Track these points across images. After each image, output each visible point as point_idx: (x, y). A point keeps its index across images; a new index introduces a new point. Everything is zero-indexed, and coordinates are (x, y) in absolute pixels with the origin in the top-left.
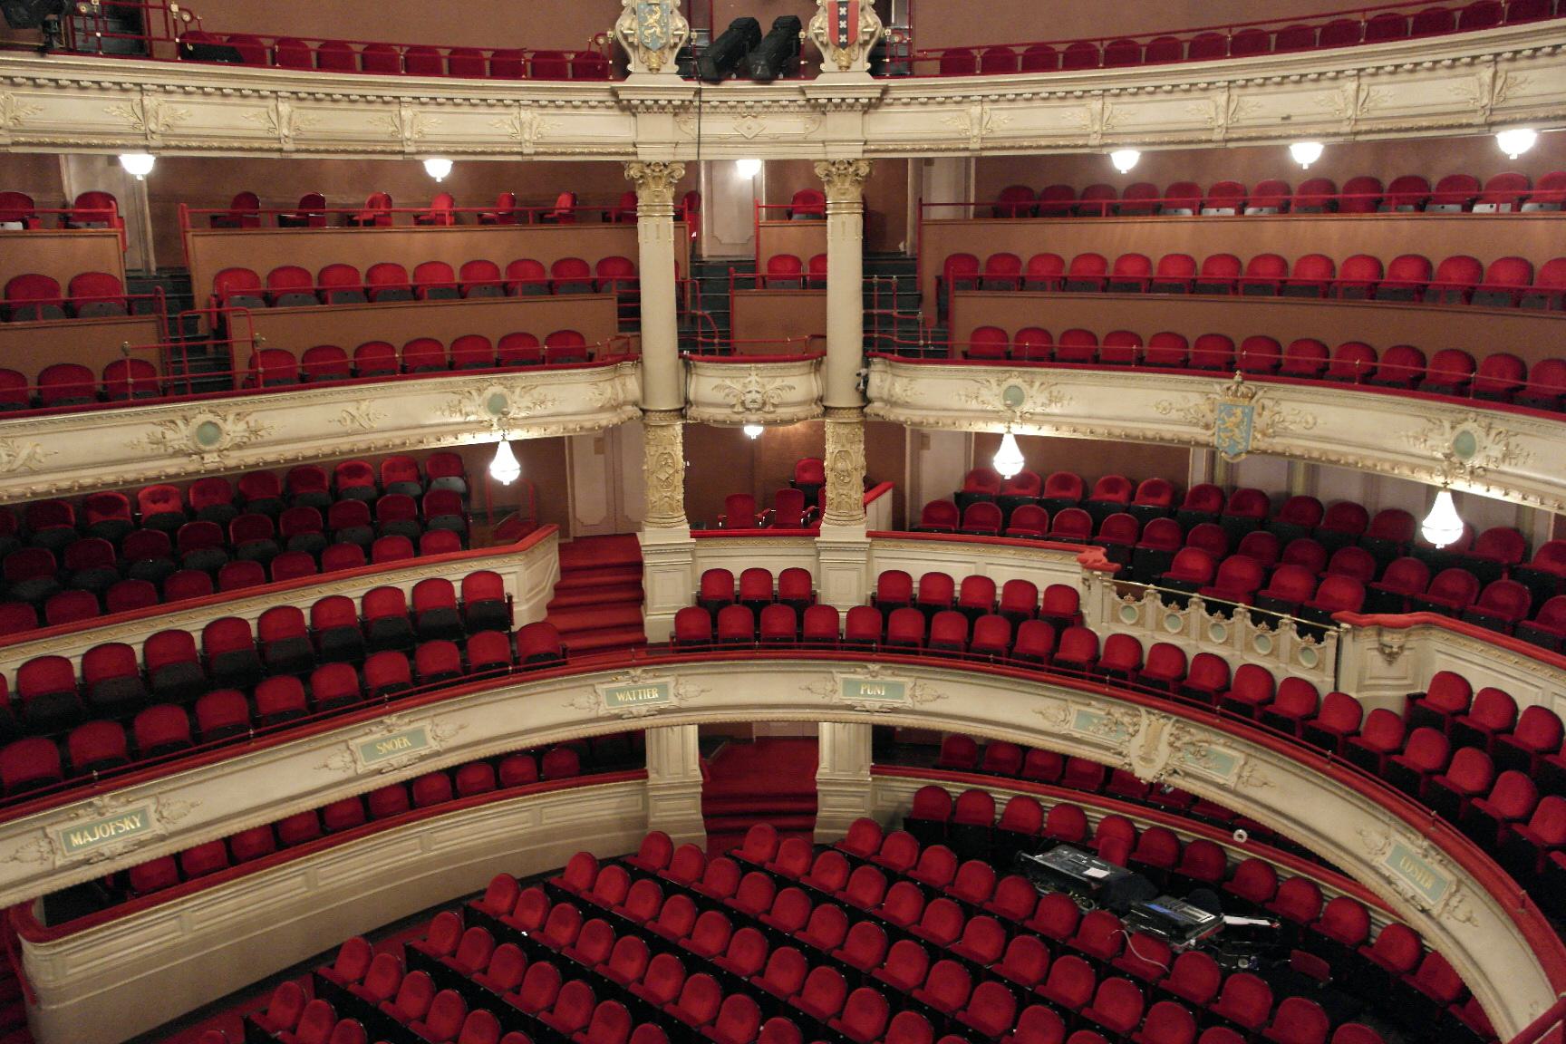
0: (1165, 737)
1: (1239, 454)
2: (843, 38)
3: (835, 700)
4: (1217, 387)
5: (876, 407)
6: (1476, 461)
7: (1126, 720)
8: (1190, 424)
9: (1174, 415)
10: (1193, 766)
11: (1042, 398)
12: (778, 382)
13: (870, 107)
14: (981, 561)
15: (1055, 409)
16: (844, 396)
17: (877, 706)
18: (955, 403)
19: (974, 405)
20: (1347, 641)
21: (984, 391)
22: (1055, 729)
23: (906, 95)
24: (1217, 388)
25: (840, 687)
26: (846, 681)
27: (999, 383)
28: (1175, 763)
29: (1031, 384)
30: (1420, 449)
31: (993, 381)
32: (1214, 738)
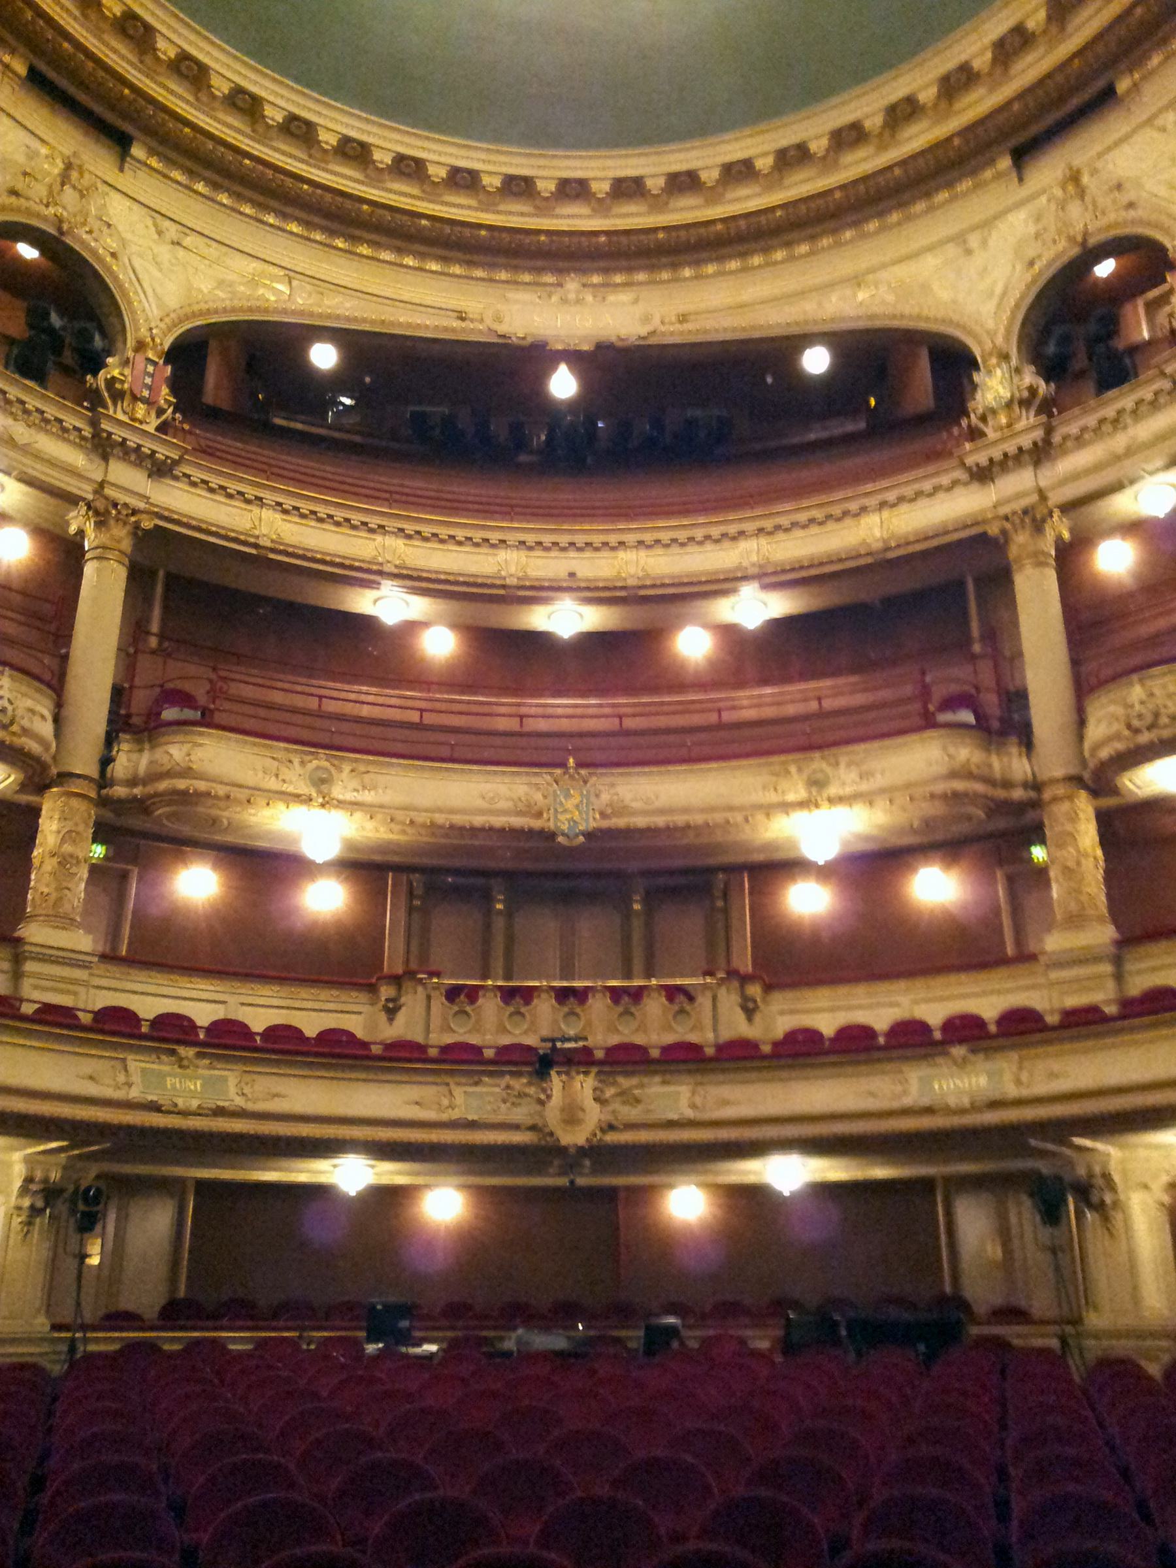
0: (588, 1093)
1: (577, 835)
2: (146, 393)
3: (134, 1094)
4: (548, 778)
5: (120, 791)
6: (833, 790)
7: (532, 1090)
8: (520, 813)
9: (503, 805)
10: (632, 1113)
11: (355, 783)
12: (29, 703)
13: (160, 470)
14: (232, 1000)
15: (367, 797)
16: (84, 762)
17: (195, 1104)
18: (249, 778)
19: (272, 784)
20: (722, 992)
21: (284, 770)
22: (444, 1117)
23: (197, 475)
24: (544, 778)
25: (136, 1078)
26: (143, 1070)
27: (302, 763)
28: (607, 1117)
29: (340, 770)
30: (772, 797)
31: (296, 761)
32: (646, 1080)
